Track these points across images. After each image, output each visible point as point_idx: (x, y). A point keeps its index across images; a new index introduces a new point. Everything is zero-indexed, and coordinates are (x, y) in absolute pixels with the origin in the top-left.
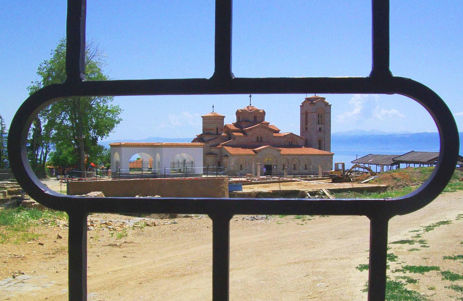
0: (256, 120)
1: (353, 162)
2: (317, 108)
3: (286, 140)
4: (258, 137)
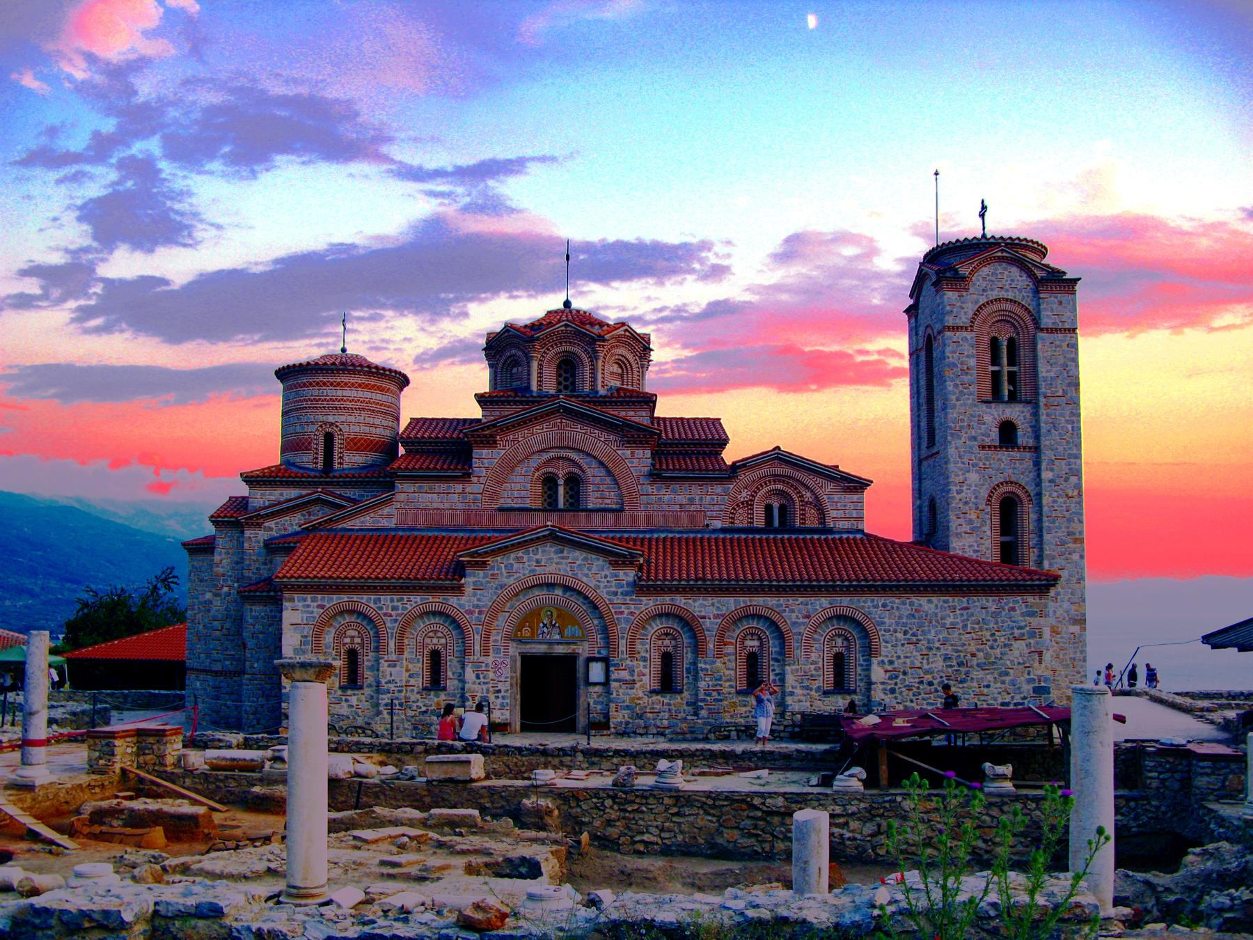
0: (573, 383)
1: (1216, 640)
2: (982, 300)
3: (745, 495)
4: (549, 482)
